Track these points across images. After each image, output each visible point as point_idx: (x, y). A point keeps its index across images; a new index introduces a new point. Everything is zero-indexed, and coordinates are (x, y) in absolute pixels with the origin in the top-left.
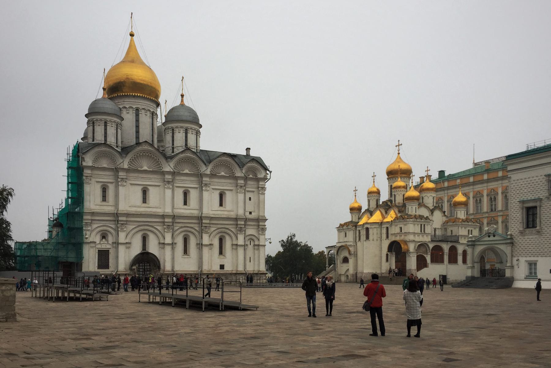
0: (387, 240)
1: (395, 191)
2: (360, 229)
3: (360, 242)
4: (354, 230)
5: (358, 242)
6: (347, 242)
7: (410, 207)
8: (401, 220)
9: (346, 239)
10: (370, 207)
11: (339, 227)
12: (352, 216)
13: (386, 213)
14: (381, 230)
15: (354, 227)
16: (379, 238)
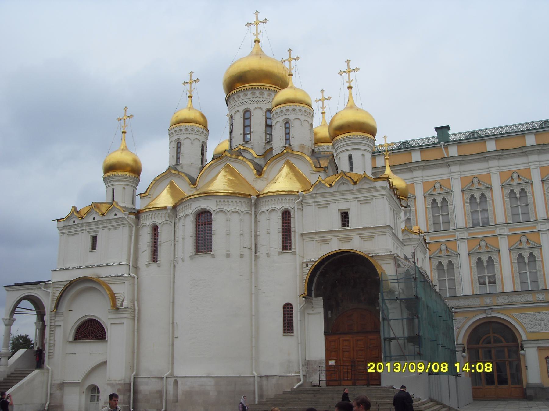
0: (287, 256)
1: (288, 110)
2: (158, 221)
3: (159, 266)
4: (130, 227)
5: (147, 265)
6: (99, 266)
7: (356, 155)
8: (343, 188)
9: (93, 259)
10: (182, 161)
11: (69, 218)
12: (113, 189)
13: (260, 172)
14: (256, 222)
15: (133, 217)
16: (251, 249)
